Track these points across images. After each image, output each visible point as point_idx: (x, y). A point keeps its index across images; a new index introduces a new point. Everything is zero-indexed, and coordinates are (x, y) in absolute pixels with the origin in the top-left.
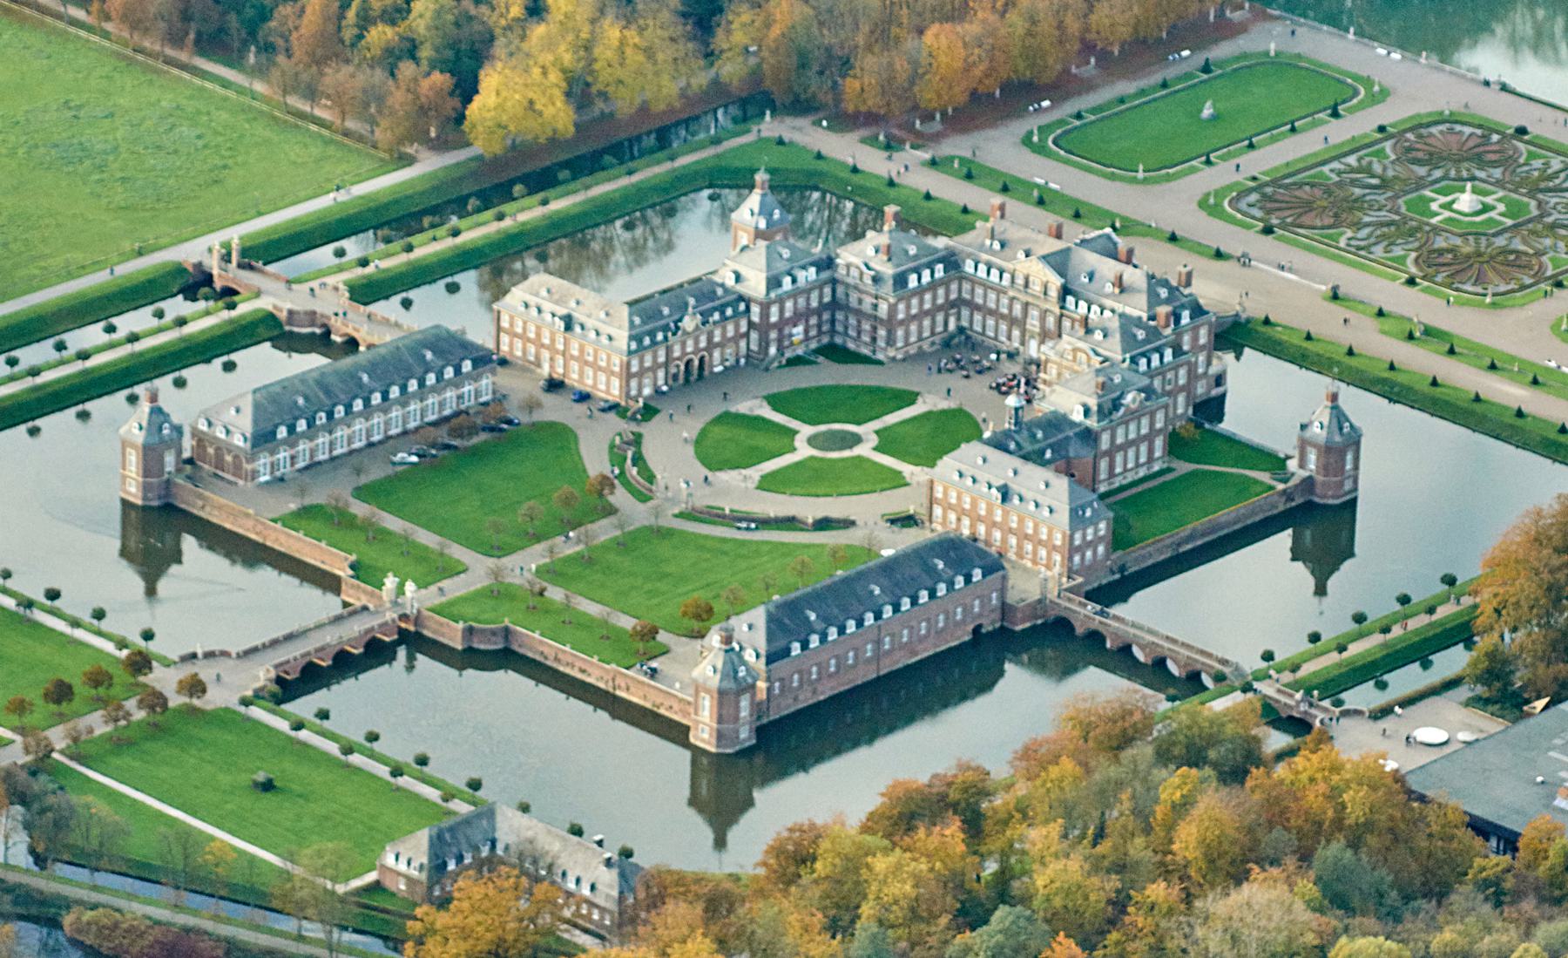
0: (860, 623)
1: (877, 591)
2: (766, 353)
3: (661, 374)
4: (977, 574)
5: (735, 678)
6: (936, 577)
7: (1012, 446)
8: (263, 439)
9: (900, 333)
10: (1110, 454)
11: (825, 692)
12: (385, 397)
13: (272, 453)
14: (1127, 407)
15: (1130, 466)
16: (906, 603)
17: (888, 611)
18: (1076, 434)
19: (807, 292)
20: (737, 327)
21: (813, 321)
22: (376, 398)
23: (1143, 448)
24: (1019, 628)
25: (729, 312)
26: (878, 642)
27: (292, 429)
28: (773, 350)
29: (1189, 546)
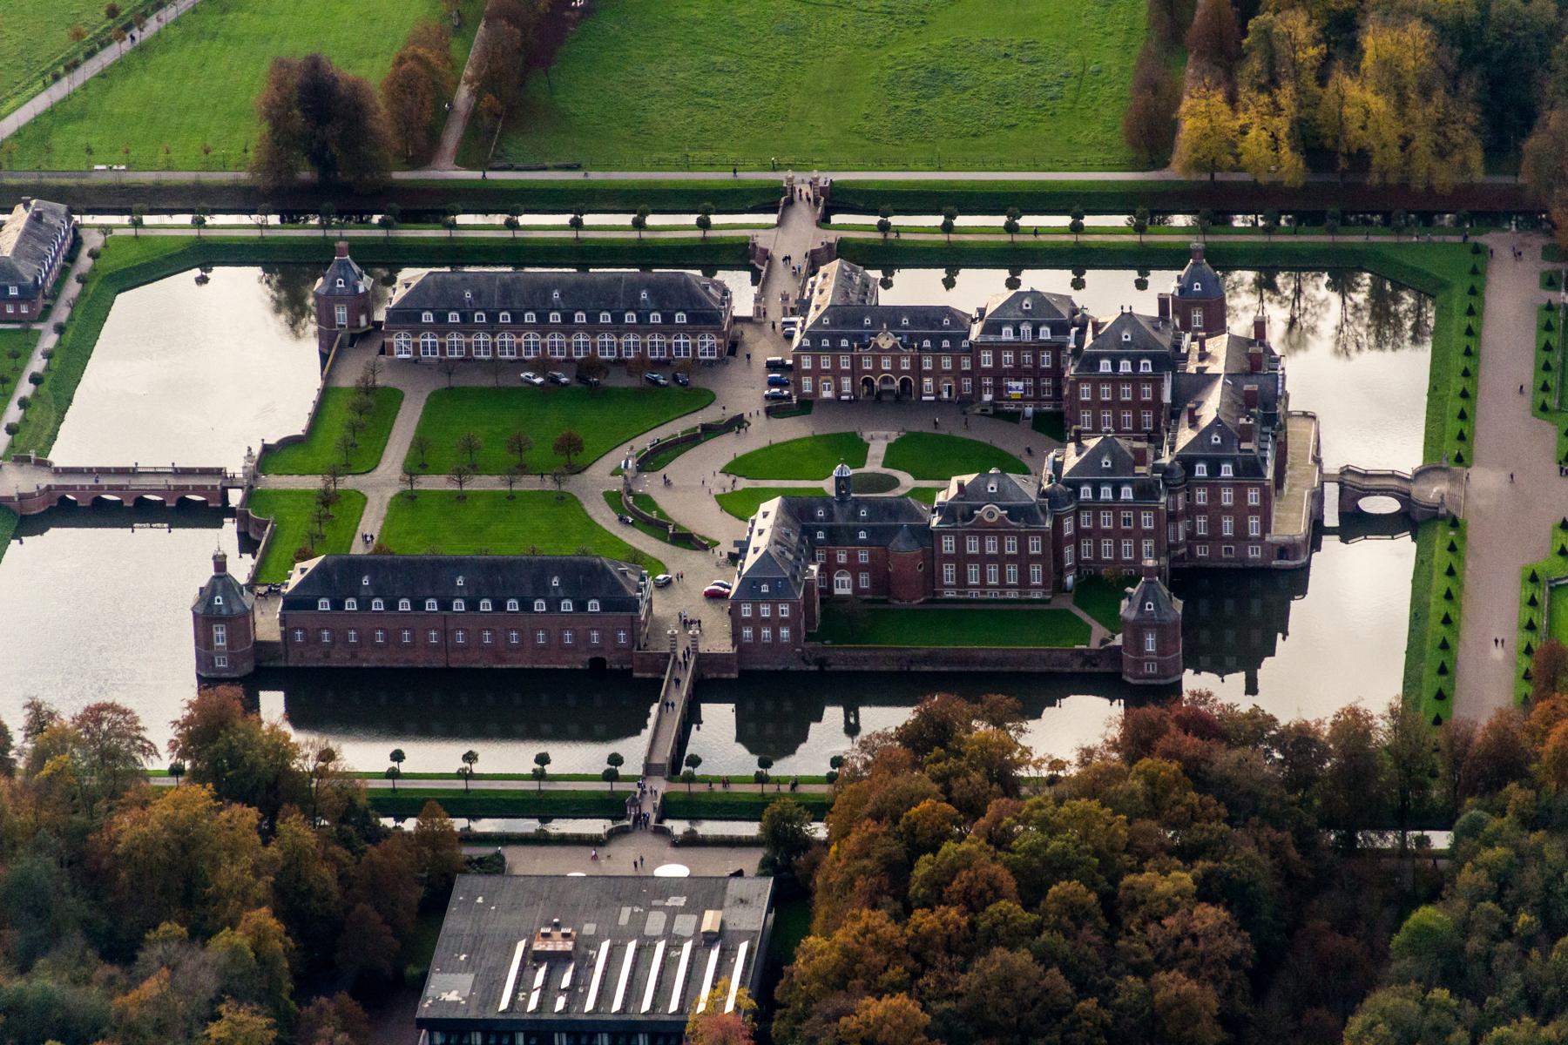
0: (418, 605)
1: (460, 581)
2: (980, 398)
3: (846, 382)
4: (594, 606)
5: (210, 604)
6: (542, 589)
7: (820, 513)
8: (405, 316)
9: (1086, 415)
10: (961, 559)
11: (370, 660)
12: (568, 318)
13: (416, 334)
14: (981, 518)
15: (986, 582)
16: (486, 605)
17: (459, 605)
18: (911, 528)
19: (1037, 348)
20: (956, 363)
21: (1047, 383)
22: (555, 317)
23: (1012, 570)
24: (637, 675)
25: (946, 344)
26: (445, 634)
27: (441, 318)
28: (988, 397)
29: (926, 668)
